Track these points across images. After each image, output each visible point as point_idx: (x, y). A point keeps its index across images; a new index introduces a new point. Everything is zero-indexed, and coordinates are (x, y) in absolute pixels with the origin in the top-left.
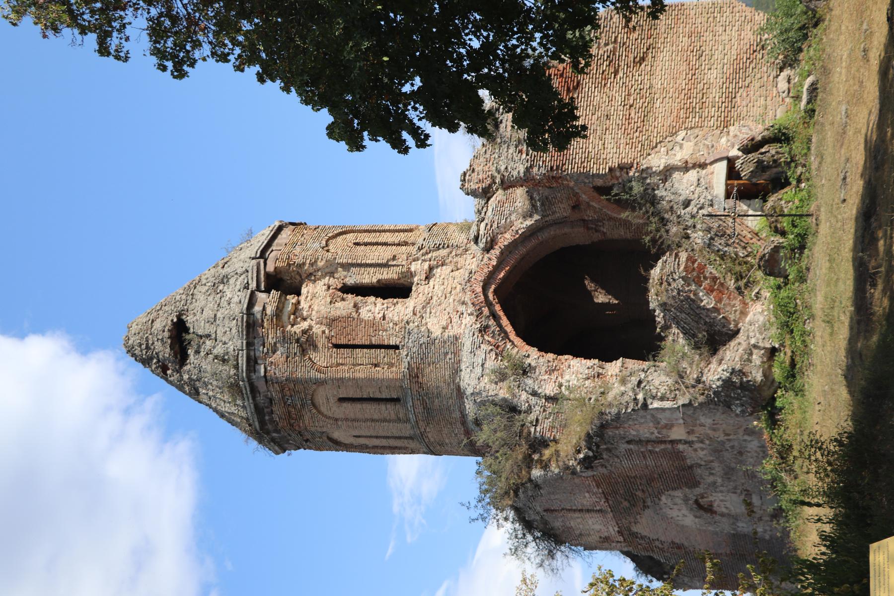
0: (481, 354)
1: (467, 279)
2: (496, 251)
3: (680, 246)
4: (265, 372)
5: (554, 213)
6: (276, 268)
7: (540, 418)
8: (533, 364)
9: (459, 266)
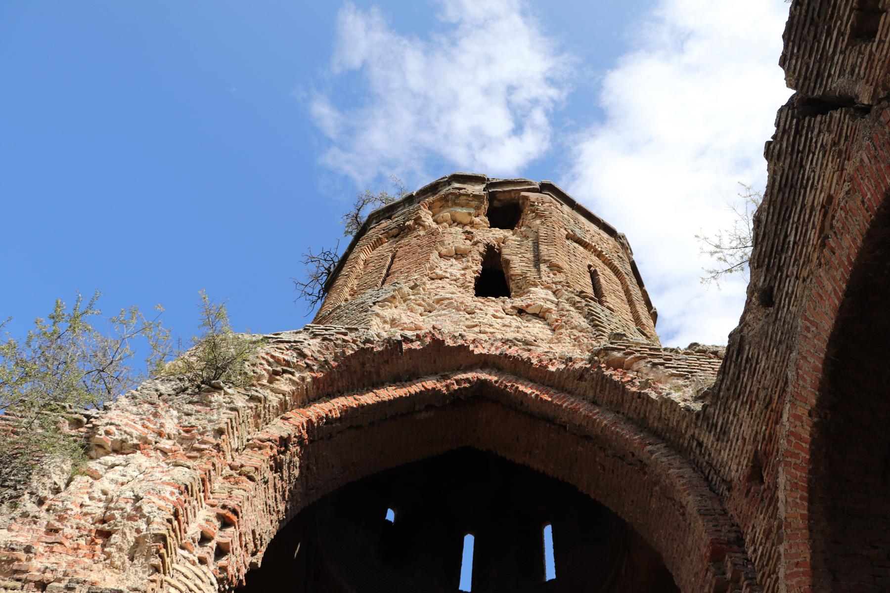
6: (527, 198)
8: (216, 398)
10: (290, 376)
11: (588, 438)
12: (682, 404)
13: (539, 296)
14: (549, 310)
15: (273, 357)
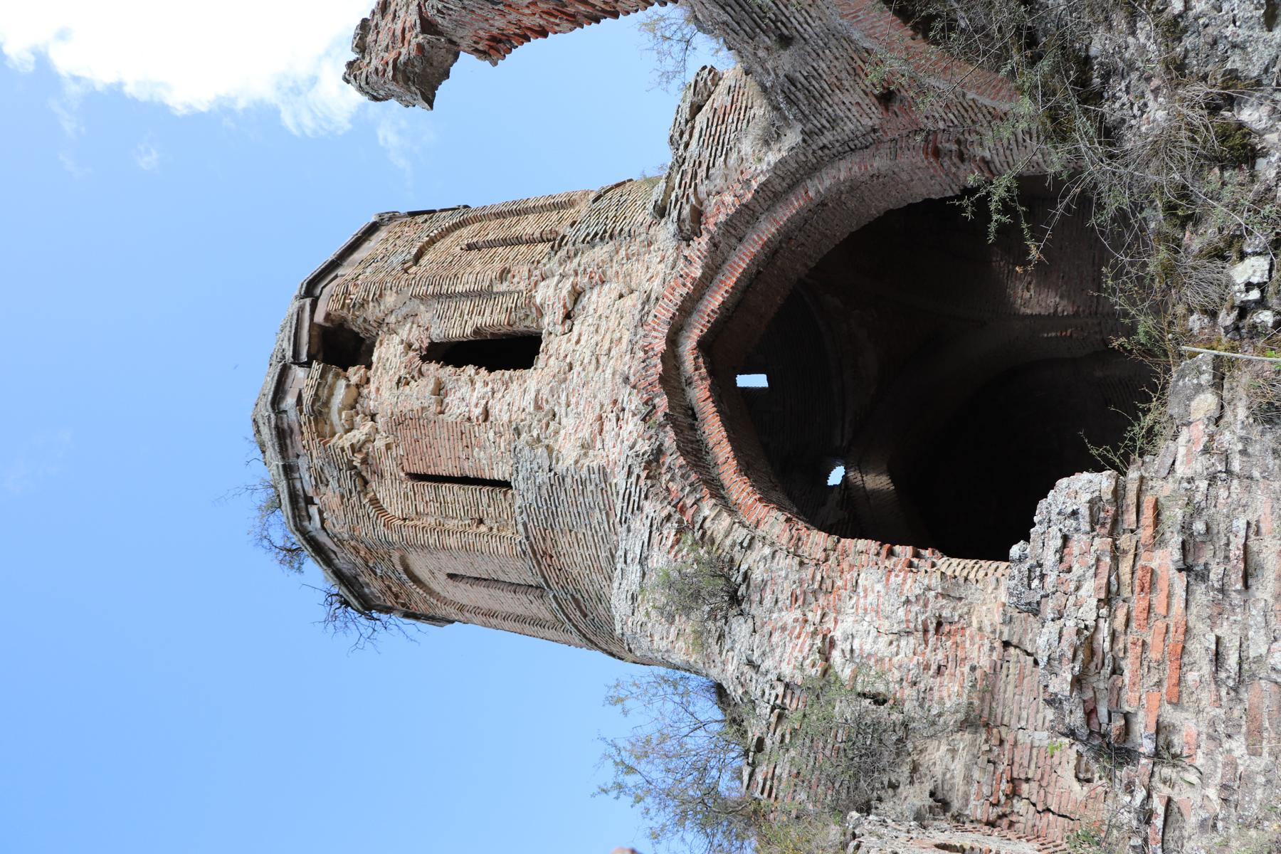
0: (640, 525)
1: (637, 317)
2: (702, 243)
3: (1192, 220)
4: (323, 521)
5: (833, 121)
6: (328, 315)
7: (768, 742)
9: (633, 286)
10: (708, 520)
11: (775, 253)
12: (785, 154)
13: (551, 294)
14: (574, 286)
15: (672, 547)
